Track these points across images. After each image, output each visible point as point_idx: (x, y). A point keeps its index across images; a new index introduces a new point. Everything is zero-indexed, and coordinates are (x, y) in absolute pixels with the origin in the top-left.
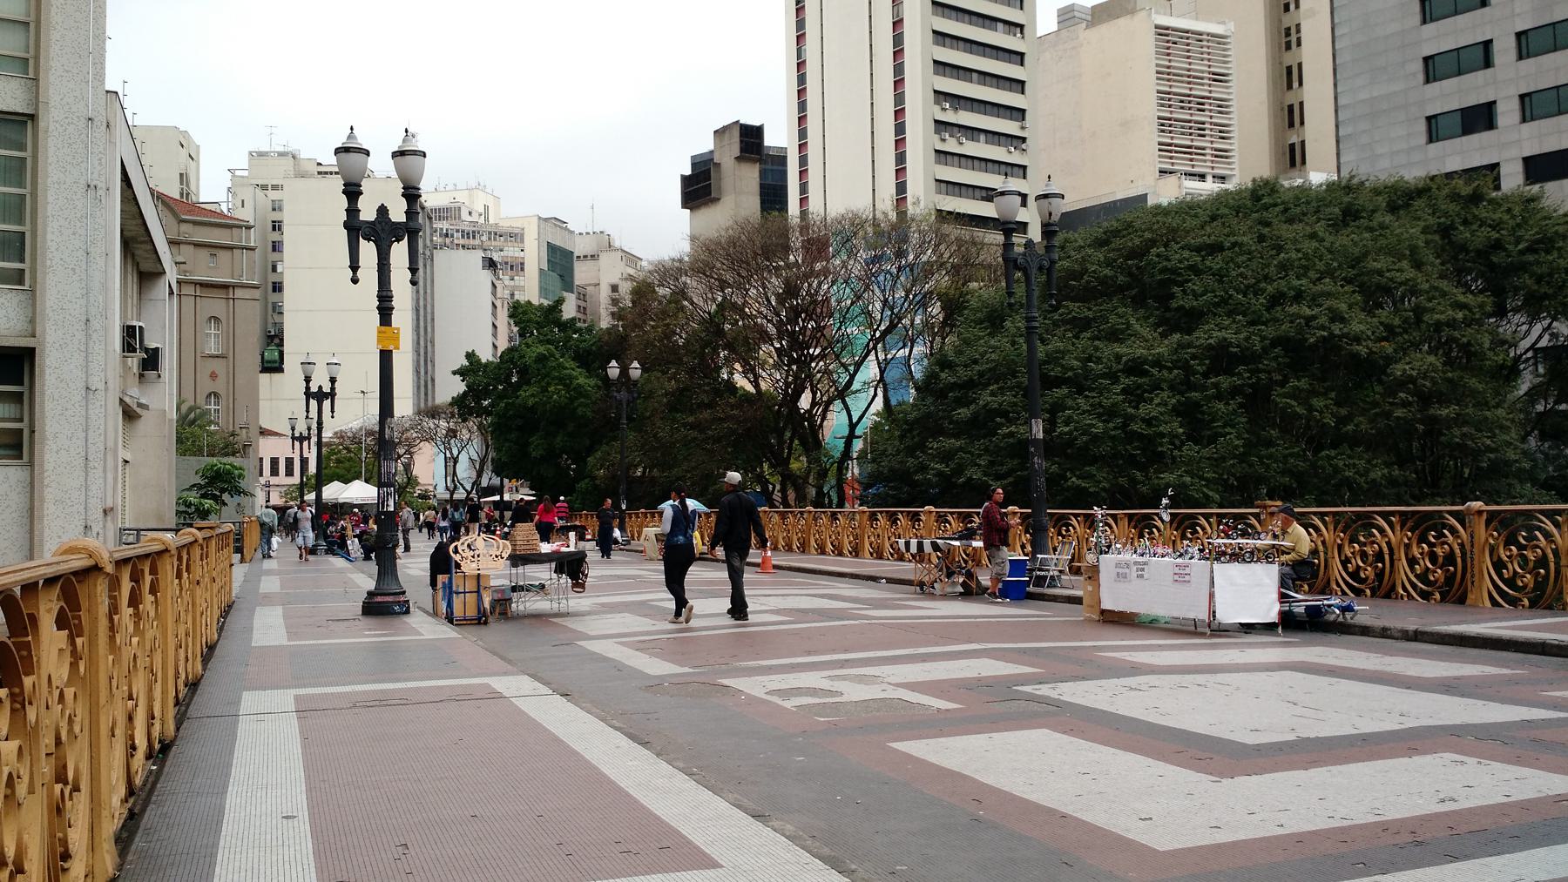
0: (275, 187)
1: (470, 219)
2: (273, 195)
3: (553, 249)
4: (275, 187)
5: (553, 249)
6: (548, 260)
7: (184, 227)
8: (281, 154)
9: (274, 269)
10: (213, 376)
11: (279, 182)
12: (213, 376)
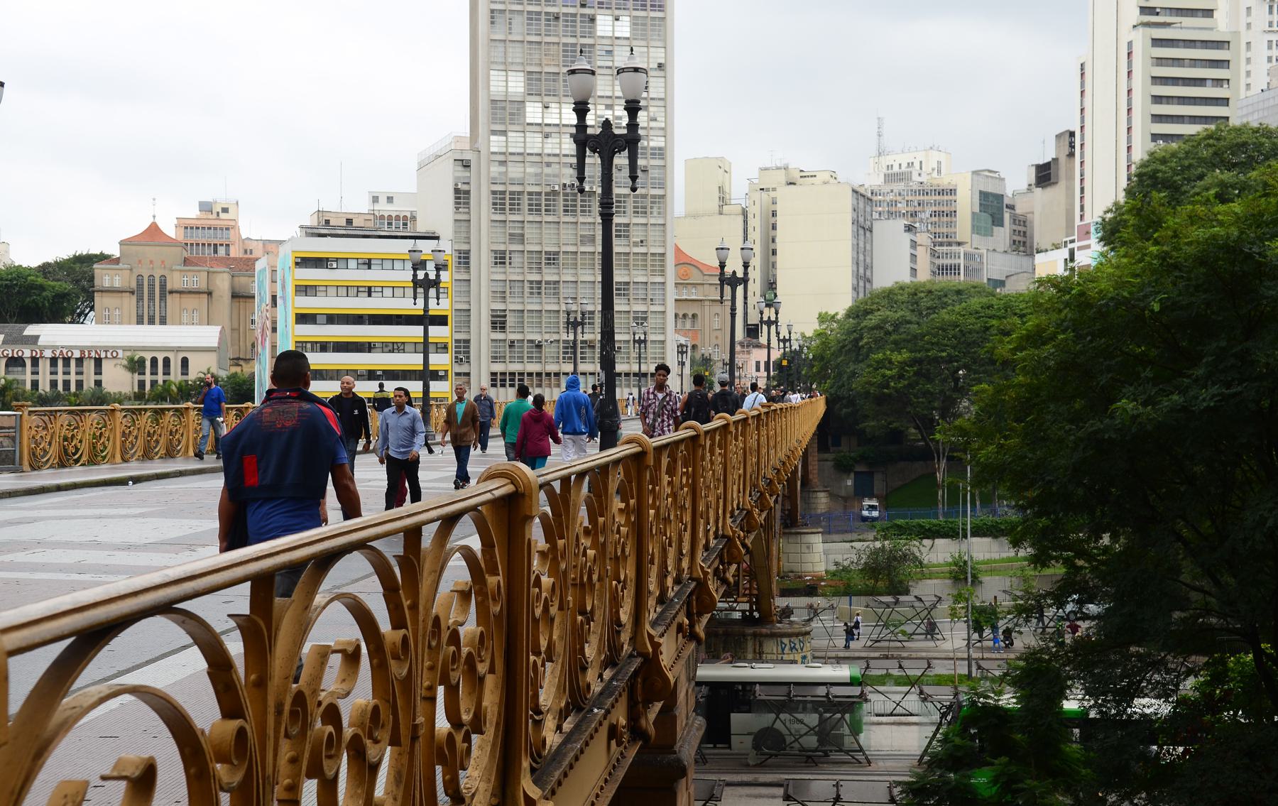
0: (774, 189)
1: (920, 179)
2: (772, 194)
3: (984, 195)
4: (774, 189)
5: (984, 195)
6: (981, 204)
7: (706, 277)
8: (778, 168)
9: (773, 241)
10: (717, 338)
11: (774, 186)
12: (717, 338)
